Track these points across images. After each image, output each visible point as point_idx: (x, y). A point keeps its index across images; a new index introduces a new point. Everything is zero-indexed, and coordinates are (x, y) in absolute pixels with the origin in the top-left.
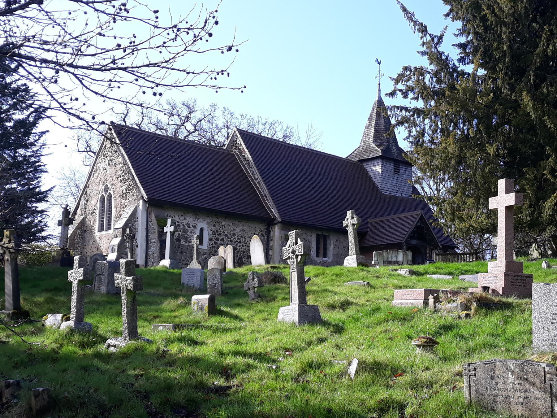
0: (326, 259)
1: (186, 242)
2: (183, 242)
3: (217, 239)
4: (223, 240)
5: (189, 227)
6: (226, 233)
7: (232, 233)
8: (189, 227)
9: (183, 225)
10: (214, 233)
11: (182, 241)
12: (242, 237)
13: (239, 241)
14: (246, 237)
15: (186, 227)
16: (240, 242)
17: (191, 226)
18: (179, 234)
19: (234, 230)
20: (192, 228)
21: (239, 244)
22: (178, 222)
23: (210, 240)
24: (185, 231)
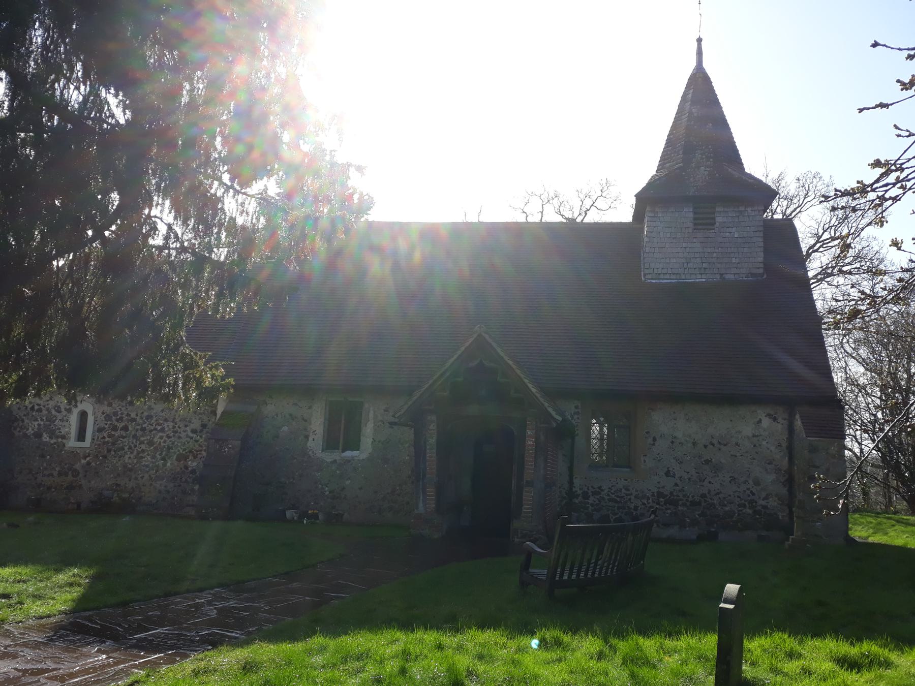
0: (356, 453)
1: (51, 438)
2: (45, 438)
3: (115, 428)
4: (125, 428)
5: (60, 412)
6: (133, 415)
7: (146, 414)
8: (60, 412)
9: (48, 410)
10: (108, 417)
11: (45, 435)
12: (166, 420)
13: (159, 428)
14: (177, 420)
15: (53, 412)
16: (162, 430)
17: (63, 410)
18: (39, 425)
19: (150, 408)
20: (64, 413)
21: (161, 434)
22: (38, 405)
23: (100, 430)
24: (51, 420)
